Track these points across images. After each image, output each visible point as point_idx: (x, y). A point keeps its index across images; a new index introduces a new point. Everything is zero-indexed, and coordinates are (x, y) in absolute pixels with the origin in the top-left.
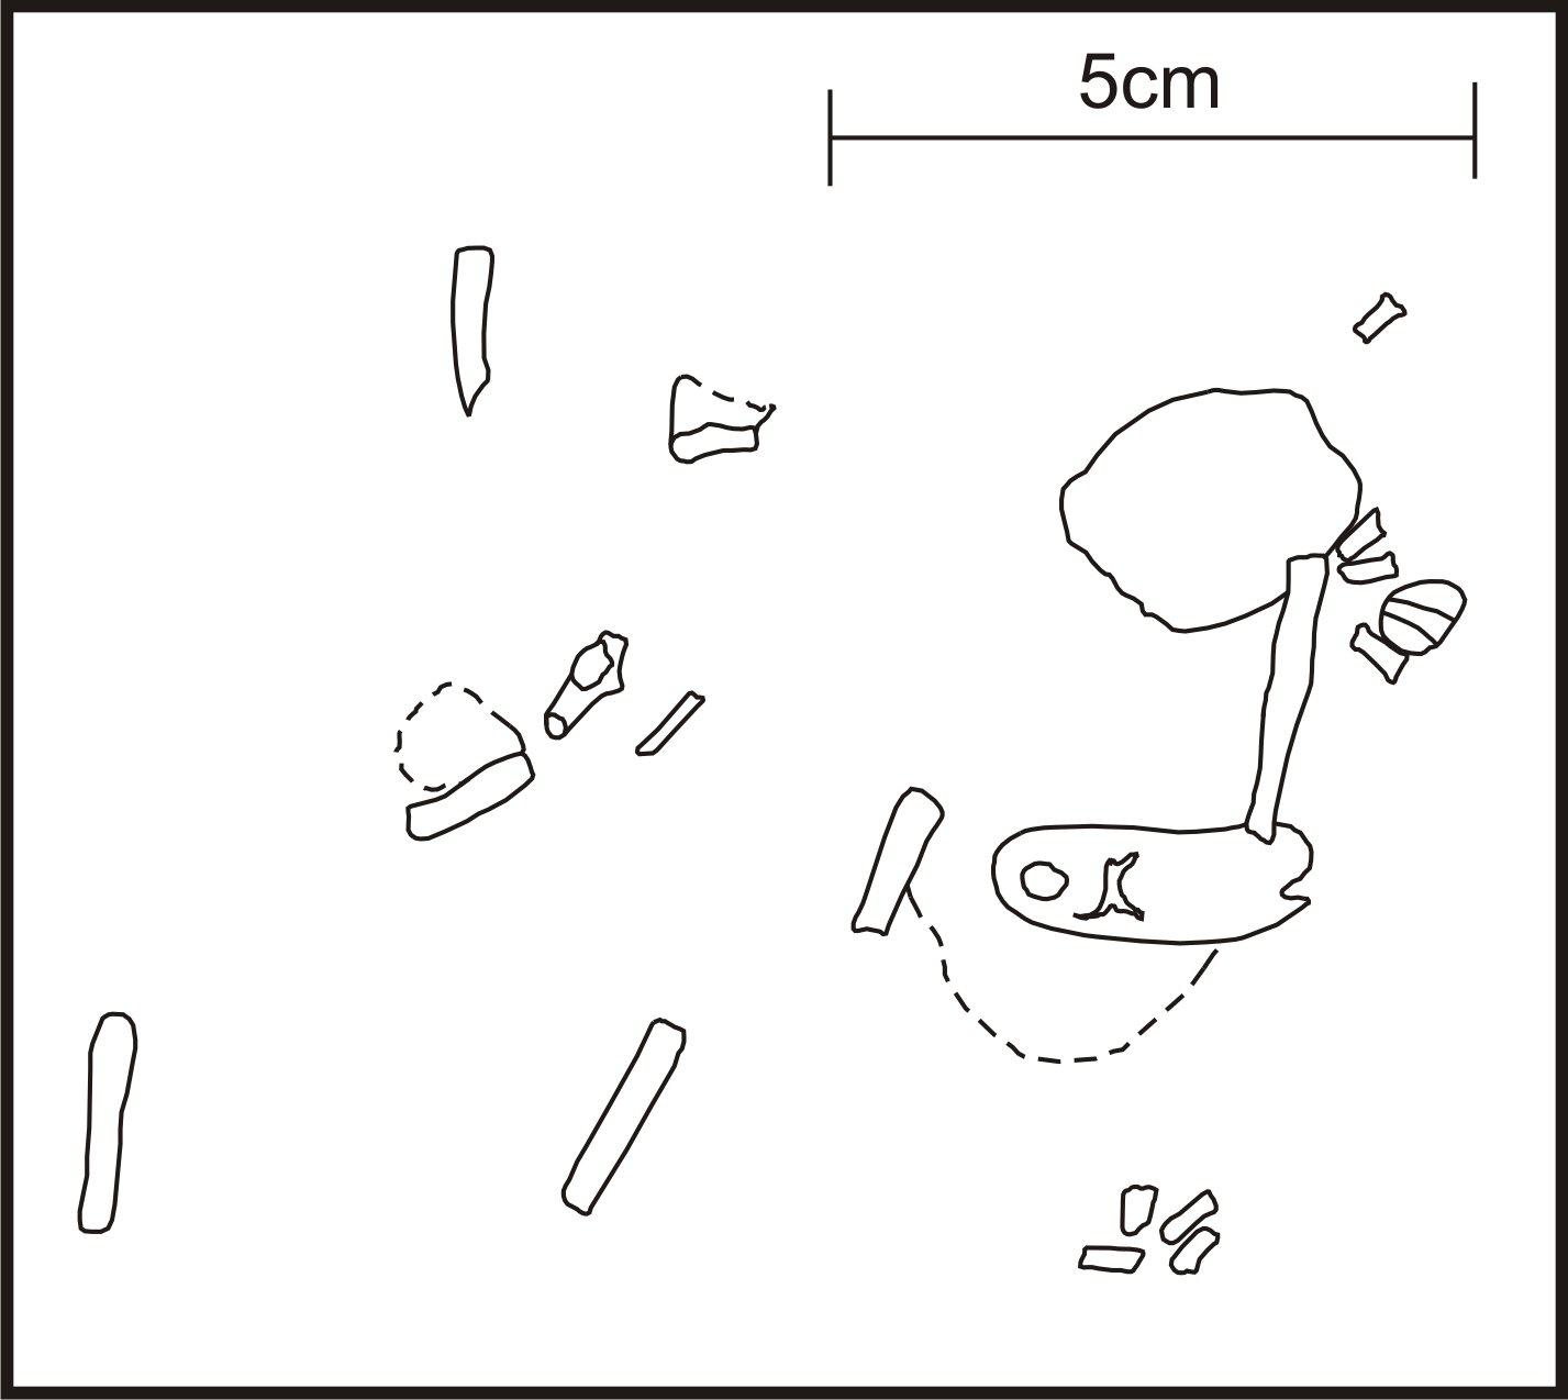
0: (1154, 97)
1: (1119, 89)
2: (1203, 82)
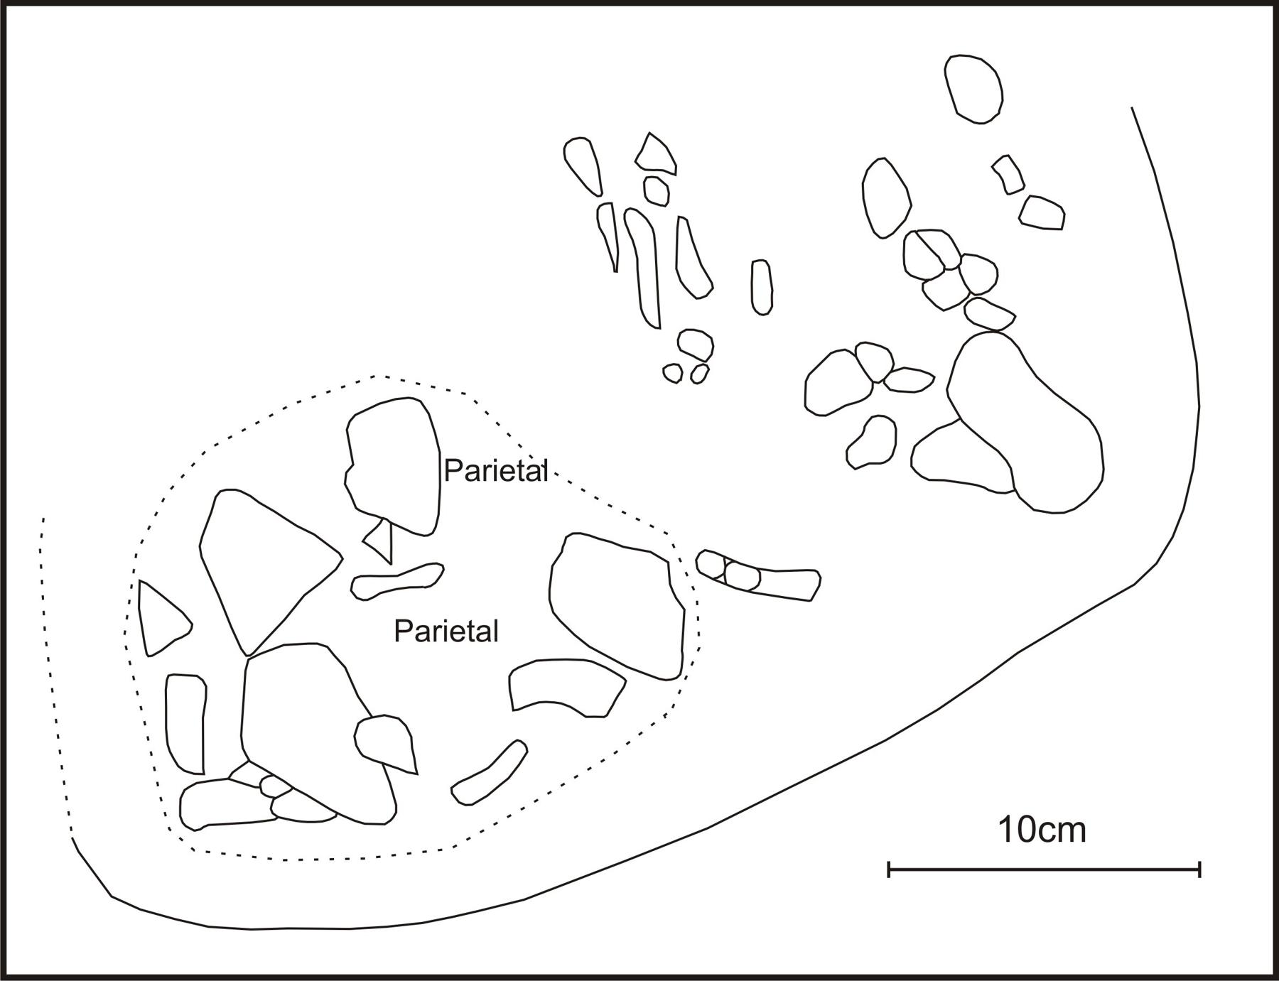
1: (1037, 831)
2: (1078, 829)
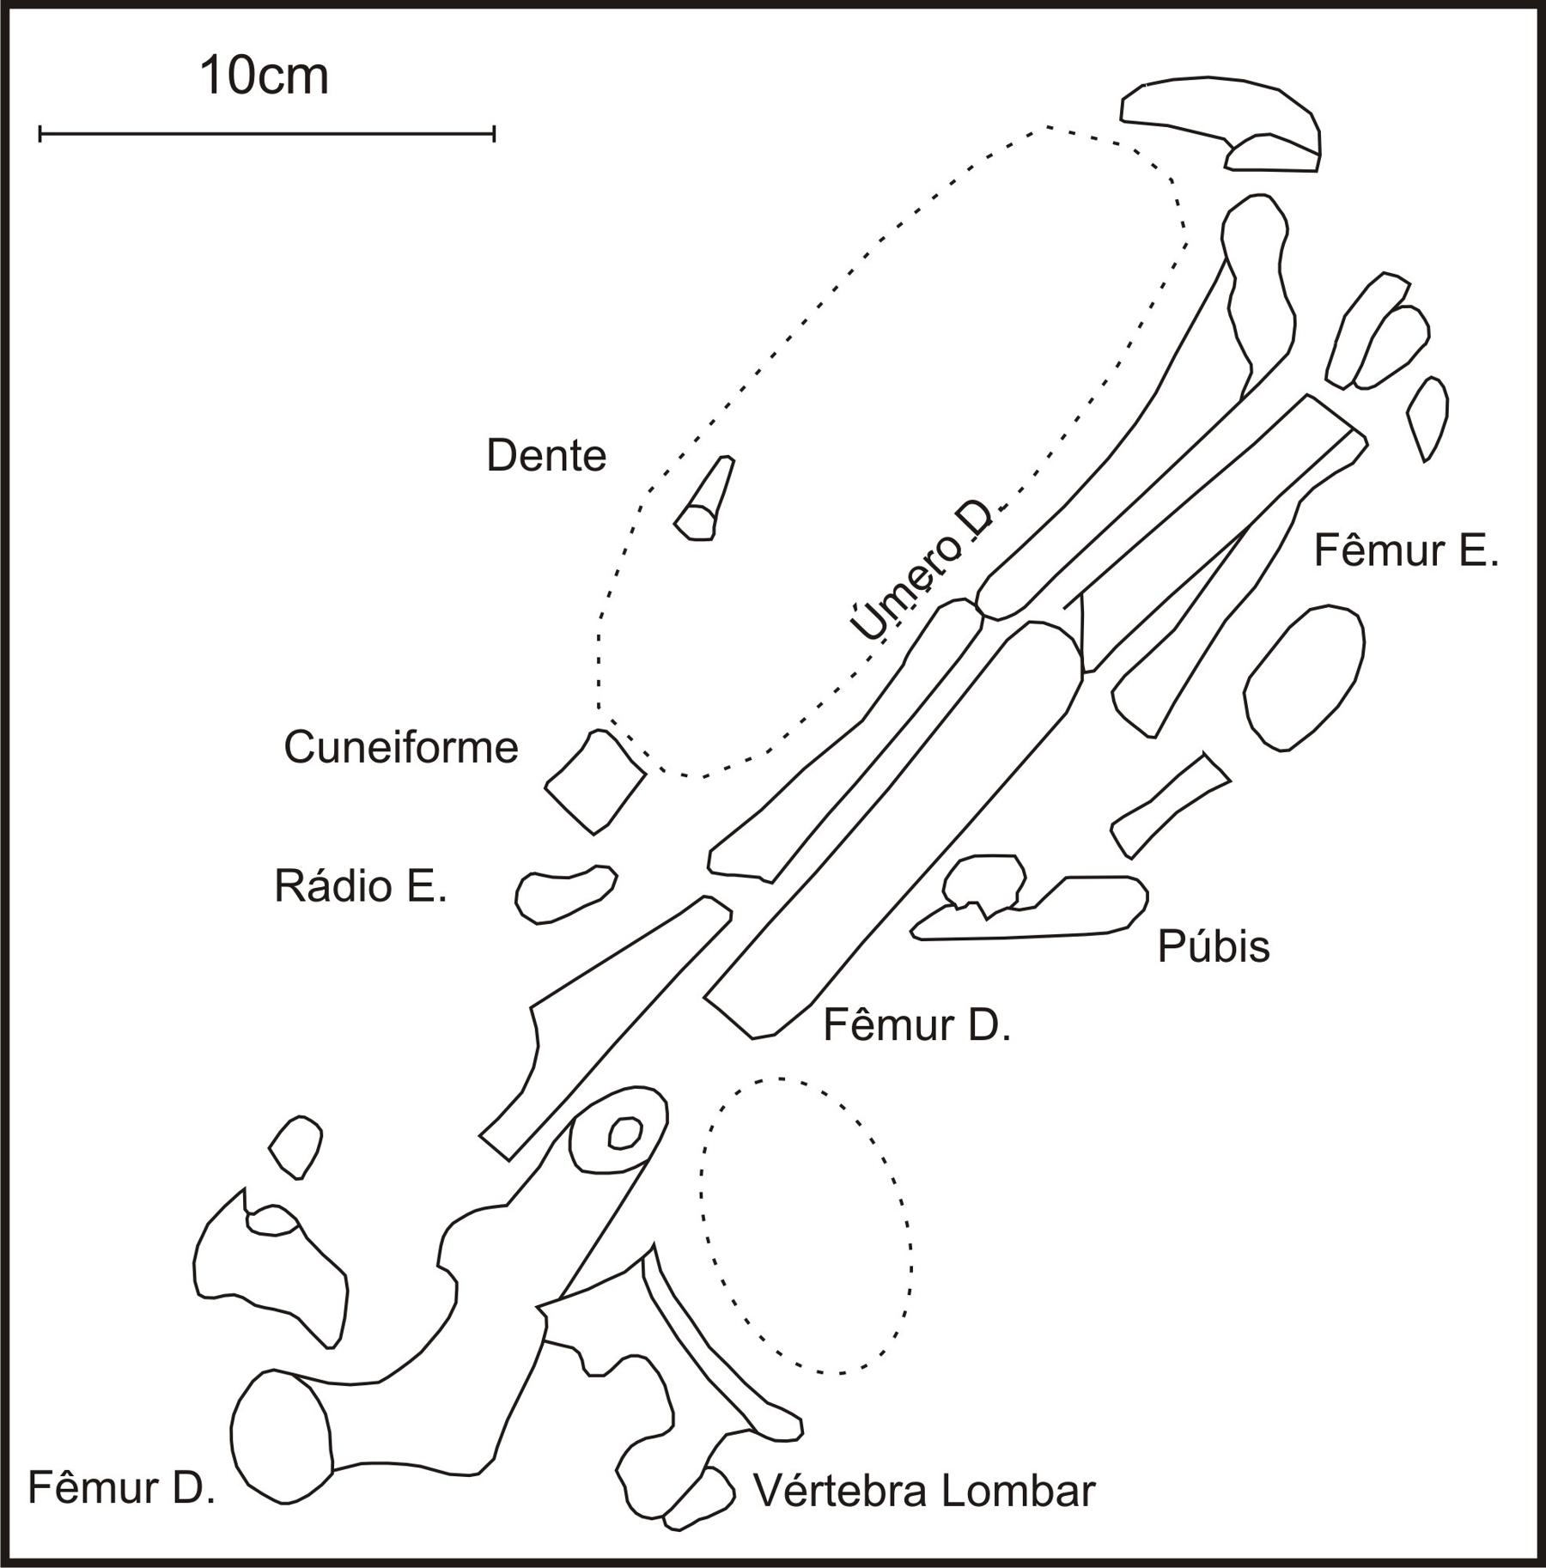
0: (281, 86)
1: (257, 77)
2: (316, 75)
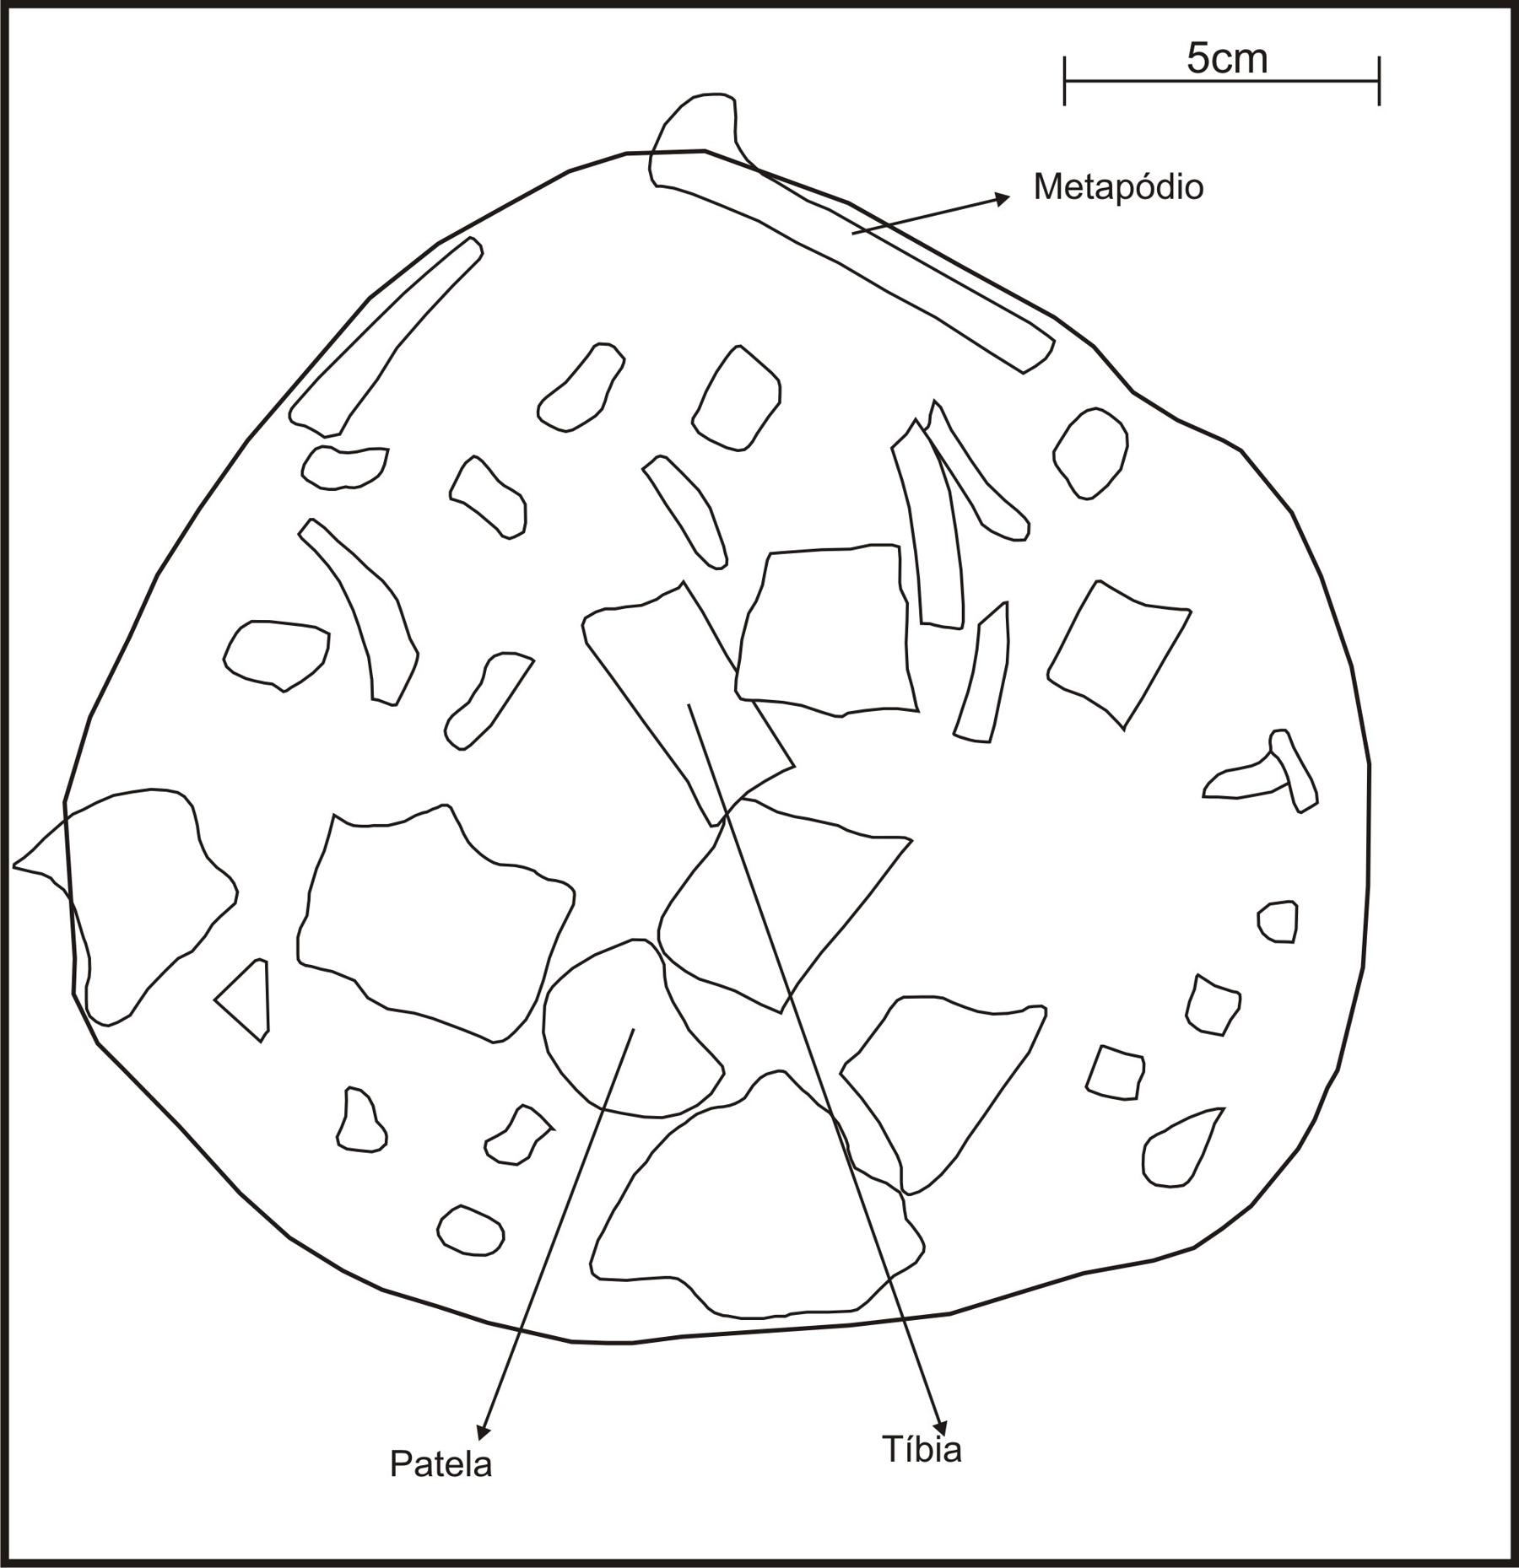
2: (1258, 58)
